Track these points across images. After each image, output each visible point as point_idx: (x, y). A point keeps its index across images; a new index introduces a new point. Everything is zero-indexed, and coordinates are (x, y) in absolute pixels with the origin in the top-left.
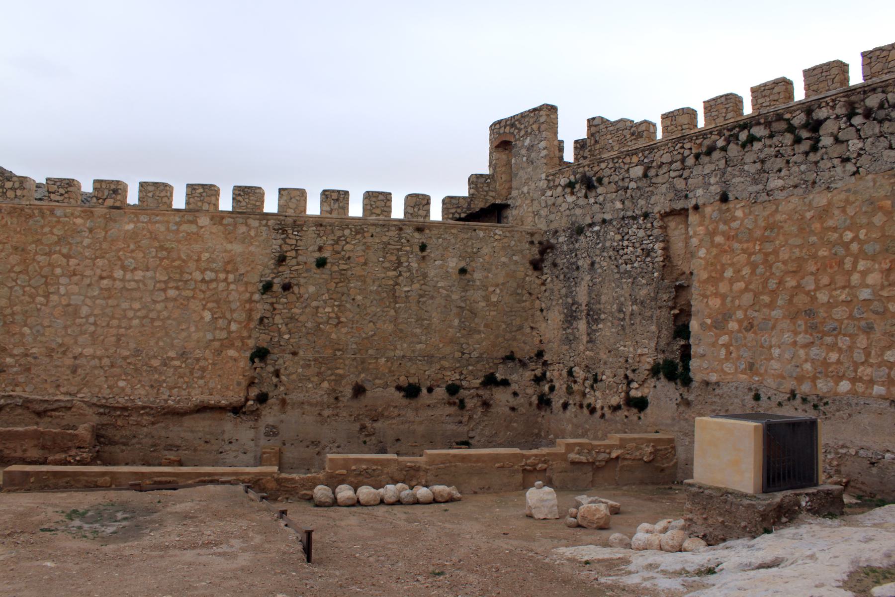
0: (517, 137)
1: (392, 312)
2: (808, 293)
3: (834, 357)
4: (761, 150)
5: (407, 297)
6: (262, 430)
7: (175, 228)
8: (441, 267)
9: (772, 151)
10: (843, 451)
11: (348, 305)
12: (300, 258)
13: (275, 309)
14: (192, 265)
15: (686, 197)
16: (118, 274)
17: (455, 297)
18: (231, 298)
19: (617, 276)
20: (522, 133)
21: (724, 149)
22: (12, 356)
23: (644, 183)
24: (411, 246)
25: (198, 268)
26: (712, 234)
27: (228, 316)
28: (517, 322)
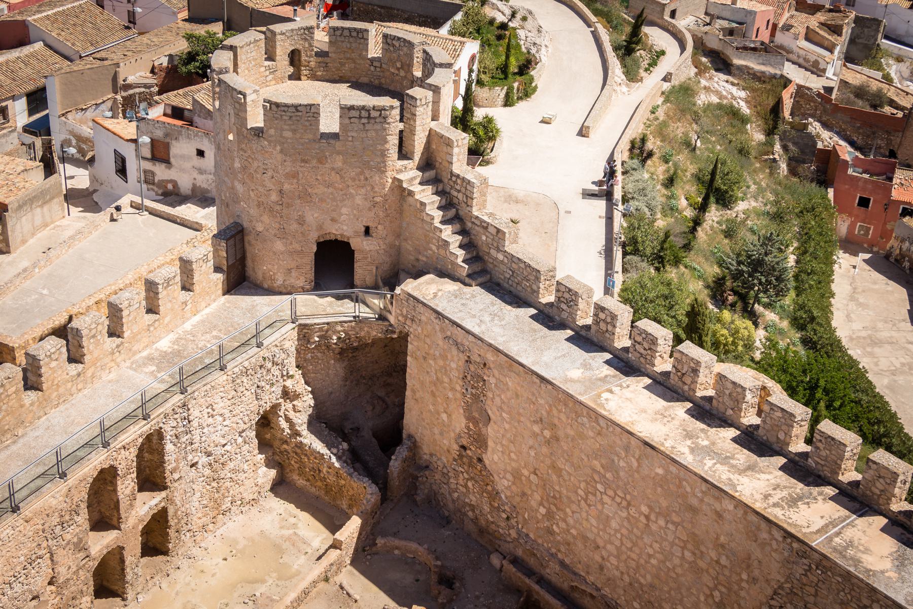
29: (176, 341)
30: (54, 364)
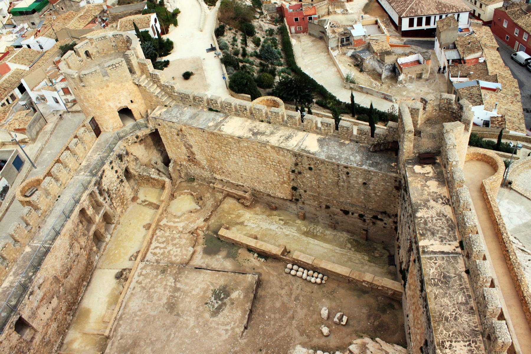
8: (356, 180)
14: (268, 160)
25: (270, 161)
28: (388, 203)
29: (87, 161)
30: (51, 185)
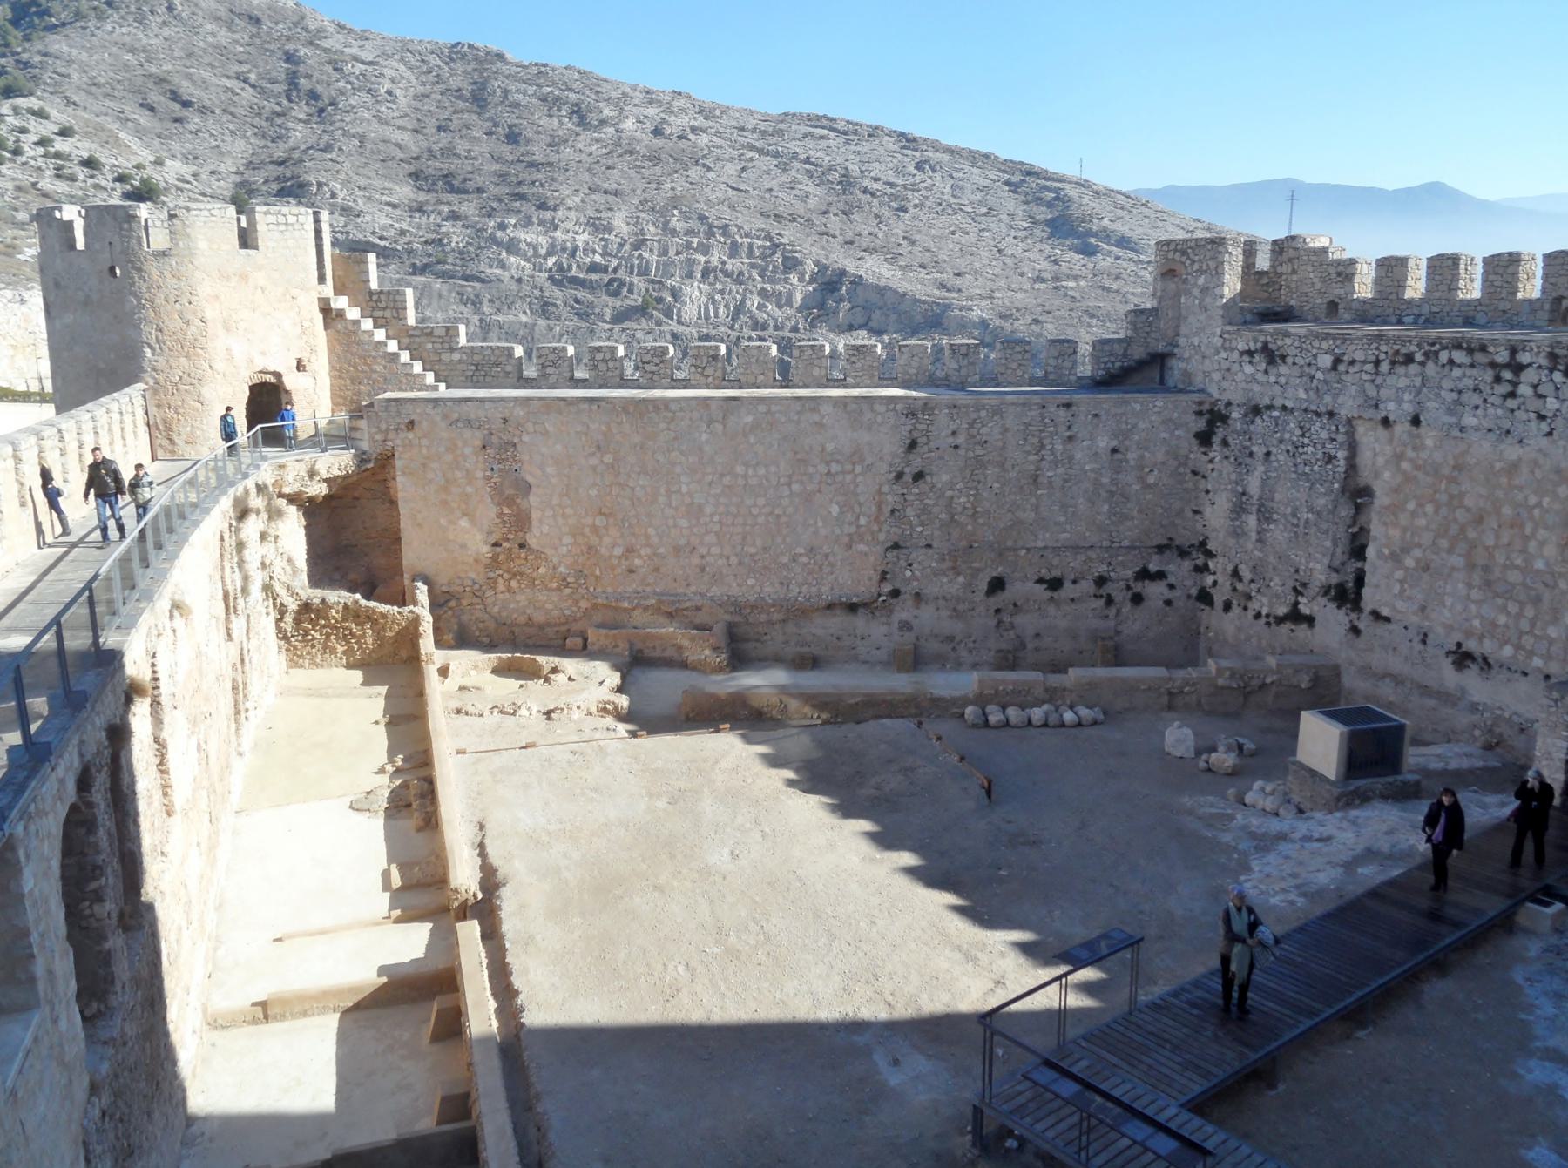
0: (1189, 270)
1: (1033, 500)
2: (1487, 548)
3: (1502, 620)
4: (1460, 379)
5: (1050, 483)
6: (896, 625)
7: (796, 418)
8: (1089, 448)
9: (1469, 383)
10: (1498, 712)
11: (985, 494)
12: (932, 445)
13: (905, 500)
15: (1377, 406)
16: (739, 469)
17: (1105, 480)
18: (859, 490)
19: (1294, 476)
20: (1196, 267)
21: (1422, 364)
22: (640, 556)
23: (1332, 376)
24: (1055, 426)
26: (1399, 457)
27: (857, 509)
28: (1177, 505)
